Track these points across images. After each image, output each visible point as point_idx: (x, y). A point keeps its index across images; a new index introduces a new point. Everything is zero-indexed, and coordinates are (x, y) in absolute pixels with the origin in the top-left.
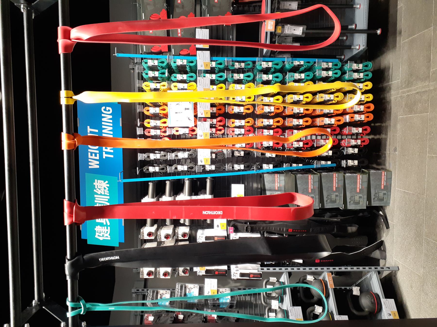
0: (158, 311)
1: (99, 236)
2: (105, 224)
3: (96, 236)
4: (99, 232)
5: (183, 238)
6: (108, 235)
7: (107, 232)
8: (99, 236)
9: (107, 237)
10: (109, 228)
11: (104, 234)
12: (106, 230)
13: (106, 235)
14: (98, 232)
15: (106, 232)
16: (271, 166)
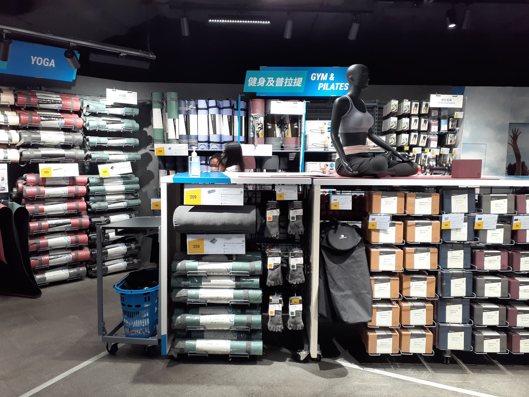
0: (52, 112)
1: (251, 79)
2: (258, 83)
3: (251, 78)
4: (253, 79)
5: (415, 160)
6: (251, 85)
7: (253, 84)
8: (251, 79)
9: (250, 84)
10: (255, 85)
11: (252, 82)
12: (254, 84)
13: (251, 83)
14: (253, 79)
15: (253, 83)
16: (309, 189)
